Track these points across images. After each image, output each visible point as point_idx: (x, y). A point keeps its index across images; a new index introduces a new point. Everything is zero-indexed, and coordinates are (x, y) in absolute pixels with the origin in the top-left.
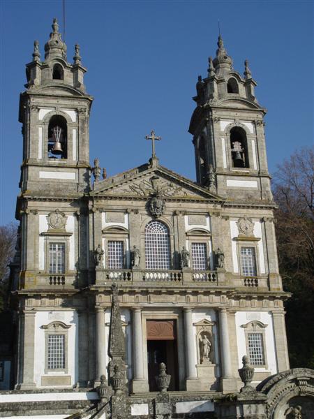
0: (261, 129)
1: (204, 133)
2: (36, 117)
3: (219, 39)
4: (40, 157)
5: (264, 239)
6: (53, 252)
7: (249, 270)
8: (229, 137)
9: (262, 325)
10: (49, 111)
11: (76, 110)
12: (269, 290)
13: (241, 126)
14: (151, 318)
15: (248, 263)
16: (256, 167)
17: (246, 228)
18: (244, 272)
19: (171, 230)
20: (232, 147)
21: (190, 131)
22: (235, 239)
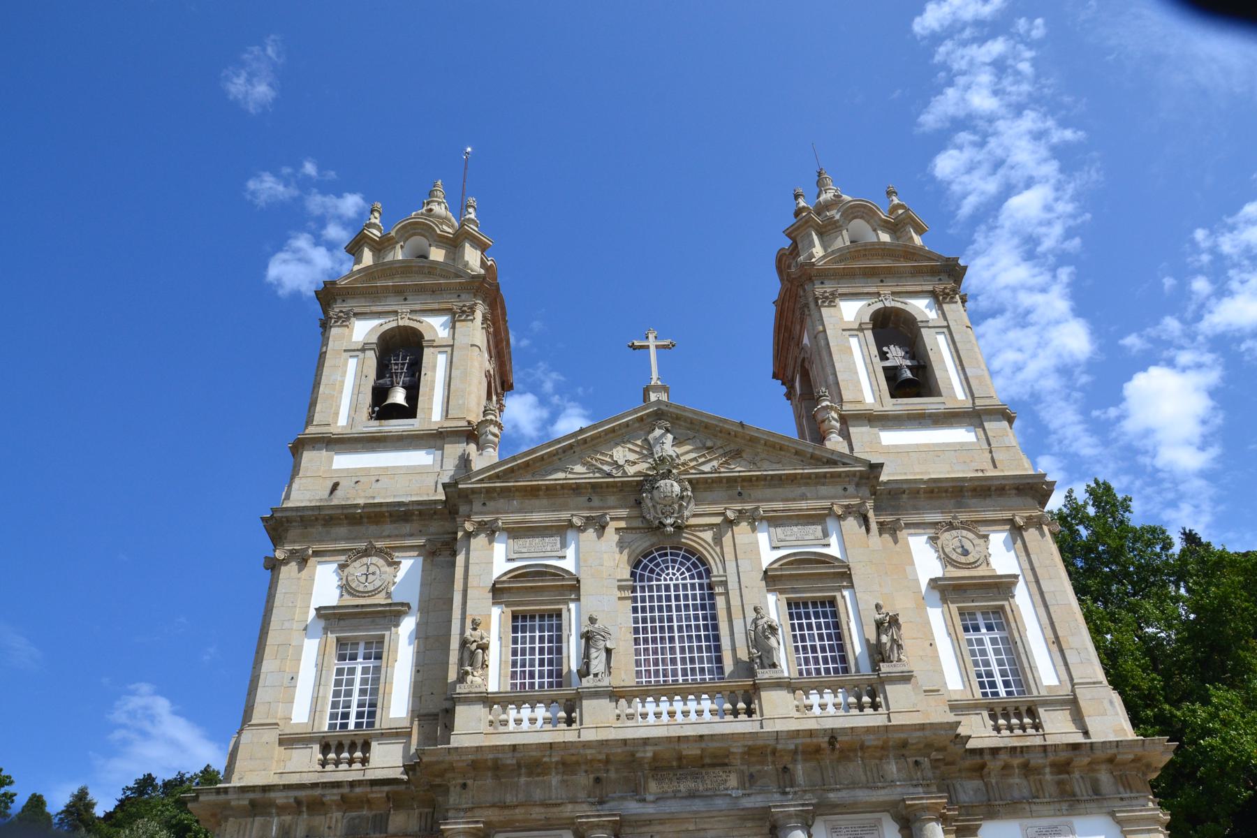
0: (955, 311)
3: (820, 174)
4: (342, 421)
5: (1031, 578)
6: (346, 665)
7: (998, 680)
8: (869, 334)
10: (375, 323)
13: (898, 305)
15: (992, 658)
16: (960, 394)
17: (966, 553)
18: (982, 685)
19: (716, 570)
20: (883, 356)
21: (775, 376)
22: (934, 583)
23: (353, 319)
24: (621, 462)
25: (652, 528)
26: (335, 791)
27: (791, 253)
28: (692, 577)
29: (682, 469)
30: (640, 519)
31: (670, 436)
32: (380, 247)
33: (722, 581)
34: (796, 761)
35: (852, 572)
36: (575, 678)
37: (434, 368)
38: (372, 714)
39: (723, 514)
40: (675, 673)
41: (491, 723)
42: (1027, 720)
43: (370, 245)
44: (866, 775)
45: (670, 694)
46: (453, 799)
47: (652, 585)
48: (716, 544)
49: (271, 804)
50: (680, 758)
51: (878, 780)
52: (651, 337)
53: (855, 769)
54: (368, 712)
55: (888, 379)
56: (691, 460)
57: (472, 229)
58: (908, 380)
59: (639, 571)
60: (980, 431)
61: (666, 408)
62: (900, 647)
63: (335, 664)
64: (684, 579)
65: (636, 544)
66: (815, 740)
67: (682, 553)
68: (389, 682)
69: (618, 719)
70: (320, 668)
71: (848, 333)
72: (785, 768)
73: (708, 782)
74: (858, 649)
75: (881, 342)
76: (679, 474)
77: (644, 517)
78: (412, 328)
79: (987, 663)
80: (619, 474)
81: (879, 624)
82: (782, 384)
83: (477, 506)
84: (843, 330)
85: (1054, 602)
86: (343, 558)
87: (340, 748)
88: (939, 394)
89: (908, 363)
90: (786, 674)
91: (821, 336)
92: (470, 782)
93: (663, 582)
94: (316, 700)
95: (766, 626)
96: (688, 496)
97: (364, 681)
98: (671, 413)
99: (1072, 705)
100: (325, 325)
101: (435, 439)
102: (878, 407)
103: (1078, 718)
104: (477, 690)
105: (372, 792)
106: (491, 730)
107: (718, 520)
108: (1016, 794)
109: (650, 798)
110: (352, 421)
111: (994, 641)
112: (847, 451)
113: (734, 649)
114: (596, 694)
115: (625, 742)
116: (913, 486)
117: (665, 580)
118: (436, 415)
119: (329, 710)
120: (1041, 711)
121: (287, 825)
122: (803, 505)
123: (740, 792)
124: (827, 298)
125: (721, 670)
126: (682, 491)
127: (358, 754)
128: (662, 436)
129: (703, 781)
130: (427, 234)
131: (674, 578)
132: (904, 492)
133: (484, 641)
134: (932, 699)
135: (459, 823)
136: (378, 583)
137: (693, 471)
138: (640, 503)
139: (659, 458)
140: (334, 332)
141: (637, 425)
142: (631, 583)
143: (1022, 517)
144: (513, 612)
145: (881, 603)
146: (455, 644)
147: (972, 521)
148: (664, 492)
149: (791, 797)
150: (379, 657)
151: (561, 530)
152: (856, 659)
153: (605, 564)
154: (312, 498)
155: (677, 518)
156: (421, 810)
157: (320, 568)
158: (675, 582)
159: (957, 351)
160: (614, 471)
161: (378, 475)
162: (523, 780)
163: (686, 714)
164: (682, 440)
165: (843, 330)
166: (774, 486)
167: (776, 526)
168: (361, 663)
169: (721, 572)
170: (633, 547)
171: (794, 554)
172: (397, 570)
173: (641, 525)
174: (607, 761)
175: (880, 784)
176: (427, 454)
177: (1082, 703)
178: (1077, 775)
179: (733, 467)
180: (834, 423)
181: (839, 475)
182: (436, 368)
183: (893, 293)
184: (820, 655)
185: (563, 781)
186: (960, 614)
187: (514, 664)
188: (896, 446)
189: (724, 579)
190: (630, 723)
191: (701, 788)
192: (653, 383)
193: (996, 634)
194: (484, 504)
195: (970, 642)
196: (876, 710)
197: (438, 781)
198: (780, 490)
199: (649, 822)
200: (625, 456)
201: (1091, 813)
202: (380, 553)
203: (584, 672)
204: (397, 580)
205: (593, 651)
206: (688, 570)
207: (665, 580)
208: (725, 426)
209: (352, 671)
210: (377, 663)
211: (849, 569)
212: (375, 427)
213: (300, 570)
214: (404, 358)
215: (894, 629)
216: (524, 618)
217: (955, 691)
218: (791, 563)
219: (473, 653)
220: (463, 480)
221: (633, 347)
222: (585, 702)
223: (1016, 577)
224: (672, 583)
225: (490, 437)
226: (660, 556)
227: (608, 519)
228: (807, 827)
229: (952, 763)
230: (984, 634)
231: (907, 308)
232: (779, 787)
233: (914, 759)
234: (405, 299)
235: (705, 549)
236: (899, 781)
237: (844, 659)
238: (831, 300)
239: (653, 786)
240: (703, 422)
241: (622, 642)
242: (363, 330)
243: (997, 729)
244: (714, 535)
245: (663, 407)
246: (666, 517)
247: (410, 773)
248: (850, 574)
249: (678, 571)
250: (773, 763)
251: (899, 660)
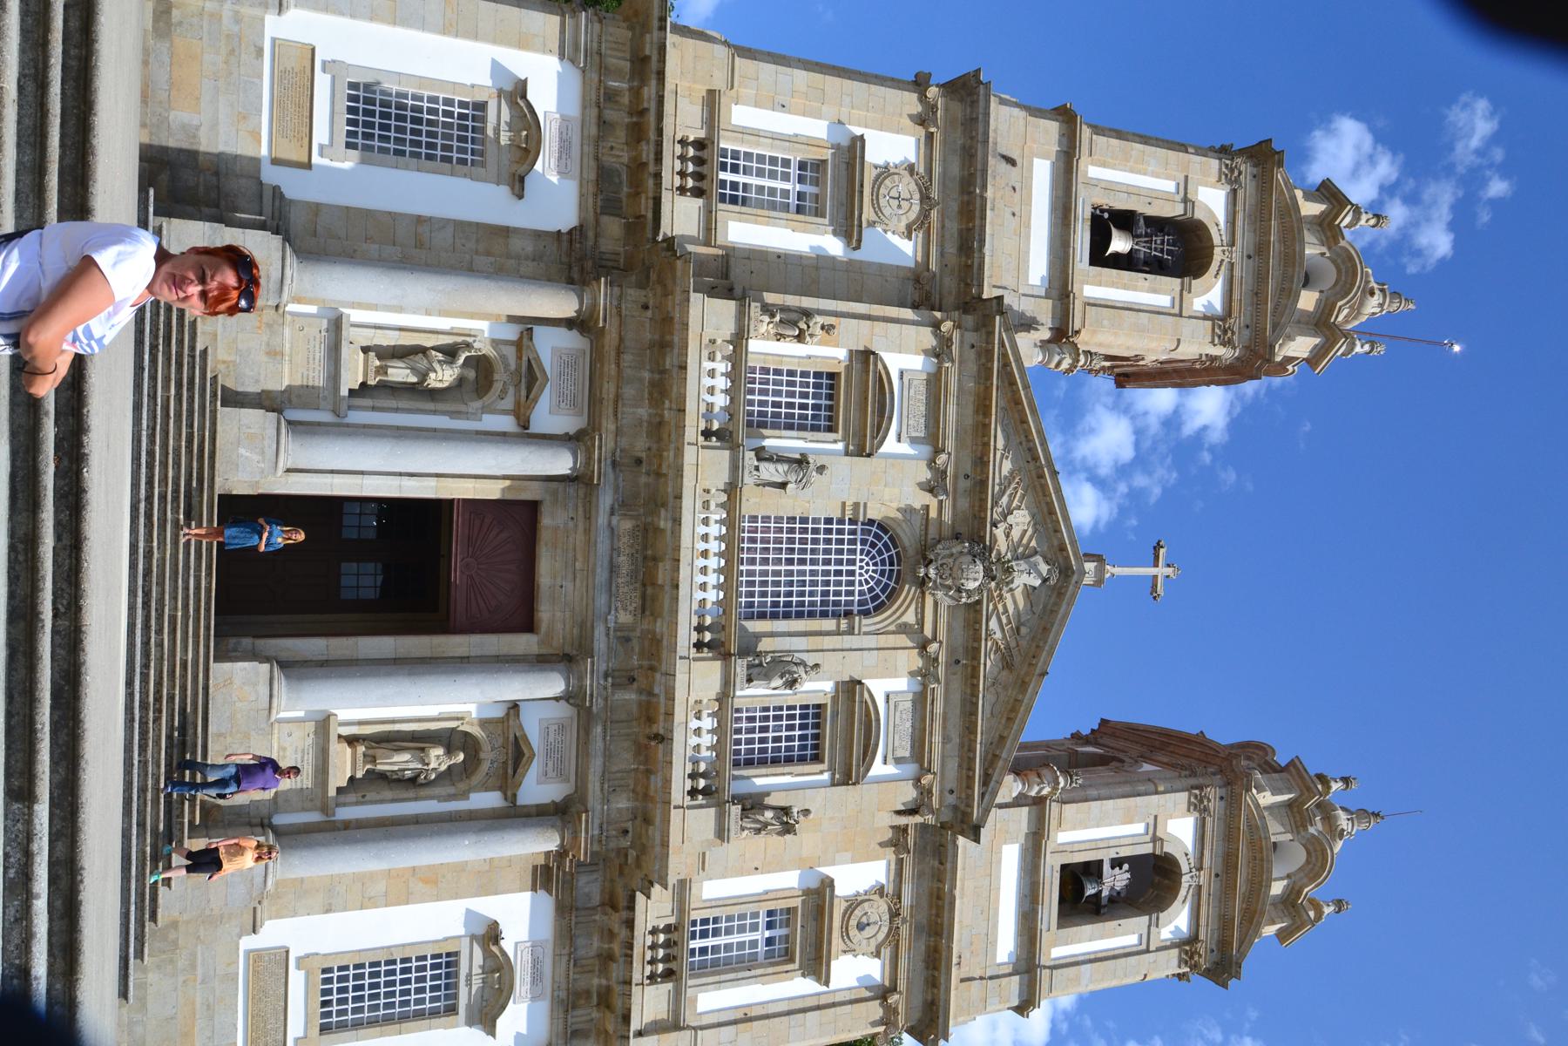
0: (1169, 964)
3: (1376, 815)
5: (823, 1000)
6: (794, 171)
7: (709, 942)
8: (1147, 849)
13: (1183, 892)
14: (546, 520)
15: (735, 938)
16: (1058, 952)
17: (861, 927)
18: (705, 922)
19: (868, 623)
20: (1117, 863)
21: (1104, 722)
22: (828, 883)
23: (1228, 188)
24: (1010, 519)
25: (925, 550)
26: (652, 156)
27: (1267, 762)
28: (861, 593)
29: (995, 594)
30: (937, 537)
31: (1037, 583)
32: (1325, 225)
33: (853, 628)
34: (641, 693)
35: (850, 787)
36: (756, 443)
37: (1154, 291)
38: (734, 200)
39: (935, 638)
40: (752, 561)
41: (713, 342)
42: (660, 967)
43: (1329, 213)
44: (618, 772)
45: (727, 555)
46: (633, 294)
47: (856, 544)
48: (900, 625)
49: (644, 82)
50: (655, 559)
51: (612, 786)
52: (1169, 571)
53: (625, 760)
54: (737, 196)
55: (1087, 865)
56: (1005, 606)
57: (1341, 348)
58: (1082, 890)
59: (874, 529)
60: (1009, 969)
61: (1073, 581)
62: (758, 831)
63: (795, 157)
64: (861, 584)
65: (907, 530)
66: (661, 718)
67: (892, 584)
68: (770, 221)
69: (704, 491)
70: (793, 140)
71: (1152, 822)
72: (634, 680)
73: (626, 590)
74: (759, 782)
75: (1136, 862)
76: (989, 590)
77: (939, 541)
78: (1209, 264)
79: (729, 931)
80: (995, 516)
81: (786, 811)
82: (1093, 731)
83: (971, 337)
84: (1156, 817)
85: (793, 1023)
86: (922, 170)
87: (699, 161)
88: (1060, 926)
89: (1105, 893)
90: (738, 693)
91: (1151, 787)
92: (649, 313)
93: (859, 557)
94: (756, 134)
95: (796, 676)
96: (961, 598)
97: (772, 191)
98: (1067, 587)
100: (1223, 152)
101: (1061, 289)
102: (1050, 846)
103: (657, 1028)
104: (752, 327)
105: (647, 198)
106: (705, 341)
107: (928, 632)
108: (580, 942)
109: (615, 520)
110: (1094, 184)
111: (754, 944)
112: (999, 800)
113: (772, 635)
114: (735, 467)
115: (679, 497)
116: (948, 876)
117: (861, 561)
118: (1091, 291)
119: (742, 149)
120: (670, 986)
121: (618, 98)
122: (937, 739)
123: (611, 625)
124: (1201, 801)
125: (750, 617)
126: (967, 591)
127: (690, 183)
128: (1039, 574)
129: (627, 584)
130: (1338, 288)
131: (863, 571)
132: (941, 863)
133: (808, 338)
134: (694, 860)
135: (605, 299)
136: (887, 211)
137: (991, 607)
138: (957, 539)
139: (1012, 567)
140: (1214, 164)
141: (1056, 543)
142: (861, 519)
143: (897, 1002)
144: (839, 374)
145: (811, 816)
146: (807, 302)
147: (898, 941)
148: (968, 569)
149: (602, 682)
150: (800, 210)
151: (932, 439)
152: (748, 778)
153: (887, 489)
154: (999, 132)
155: (935, 582)
156: (623, 256)
157: (912, 140)
158: (858, 571)
159: (1115, 957)
160: (1000, 510)
161: (1021, 217)
162: (647, 375)
163: (704, 570)
164: (1032, 597)
165: (1156, 817)
166: (963, 704)
167: (914, 702)
168: (794, 189)
169: (864, 629)
170: (904, 525)
171: (878, 720)
172: (902, 235)
173: (930, 537)
174: (659, 475)
175: (606, 786)
176: (1042, 278)
177: (674, 1035)
178: (595, 1014)
179: (992, 657)
180: (1036, 789)
181: (970, 787)
182: (1153, 292)
183: (1199, 887)
184: (757, 736)
185: (641, 421)
186: (789, 909)
187: (778, 372)
188: (999, 862)
189: (856, 631)
190: (699, 504)
191: (620, 580)
192: (1108, 567)
193: (761, 948)
194: (973, 346)
195: (755, 915)
196: (689, 793)
197: (653, 276)
198: (958, 711)
199: (588, 517)
200: (1017, 524)
201: (552, 1024)
202: (924, 215)
203: (762, 455)
204: (889, 235)
205: (782, 468)
206: (871, 590)
207: (861, 561)
208: (1045, 653)
209: (786, 177)
210: (793, 208)
211: (854, 784)
212: (1083, 213)
213: (911, 117)
214: (1169, 252)
215: (778, 827)
216: (831, 387)
217: (701, 889)
218: (868, 714)
219: (794, 323)
220: (1005, 322)
221: (1158, 547)
222: (727, 453)
223: (827, 983)
224: (856, 568)
225: (1056, 358)
226: (891, 557)
227: (941, 498)
228: (567, 697)
229: (621, 873)
230: (763, 933)
231: (1177, 903)
232: (613, 671)
233: (630, 830)
234: (1249, 257)
235: (894, 613)
236: (608, 809)
237: (749, 763)
238: (1198, 807)
239: (627, 525)
240: (1052, 626)
241: (793, 503)
242: (1212, 202)
243: (654, 931)
244: (910, 625)
245: (1075, 578)
246: (937, 568)
247: (665, 245)
248: (848, 784)
249: (871, 576)
250: (641, 667)
251: (743, 829)
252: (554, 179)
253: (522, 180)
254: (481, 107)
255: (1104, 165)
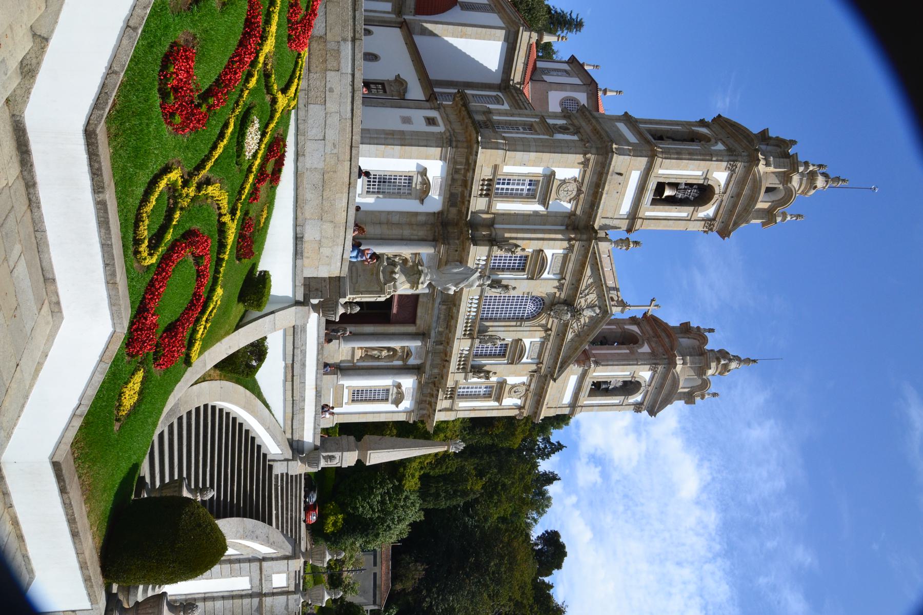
1: (642, 345)
2: (718, 170)
4: (661, 172)
5: (500, 407)
6: (527, 182)
8: (630, 379)
9: (397, 402)
11: (714, 219)
12: (440, 411)
13: (640, 391)
14: (421, 299)
17: (515, 392)
19: (527, 323)
24: (587, 297)
26: (468, 195)
49: (468, 170)
51: (433, 366)
60: (568, 406)
74: (483, 362)
86: (580, 180)
91: (635, 363)
99: (450, 409)
102: (590, 375)
108: (424, 390)
109: (440, 306)
118: (648, 214)
122: (547, 354)
127: (484, 192)
136: (562, 196)
161: (621, 194)
181: (555, 368)
183: (647, 391)
221: (653, 300)
252: (437, 197)
253: (423, 200)
254: (410, 178)
255: (667, 169)
